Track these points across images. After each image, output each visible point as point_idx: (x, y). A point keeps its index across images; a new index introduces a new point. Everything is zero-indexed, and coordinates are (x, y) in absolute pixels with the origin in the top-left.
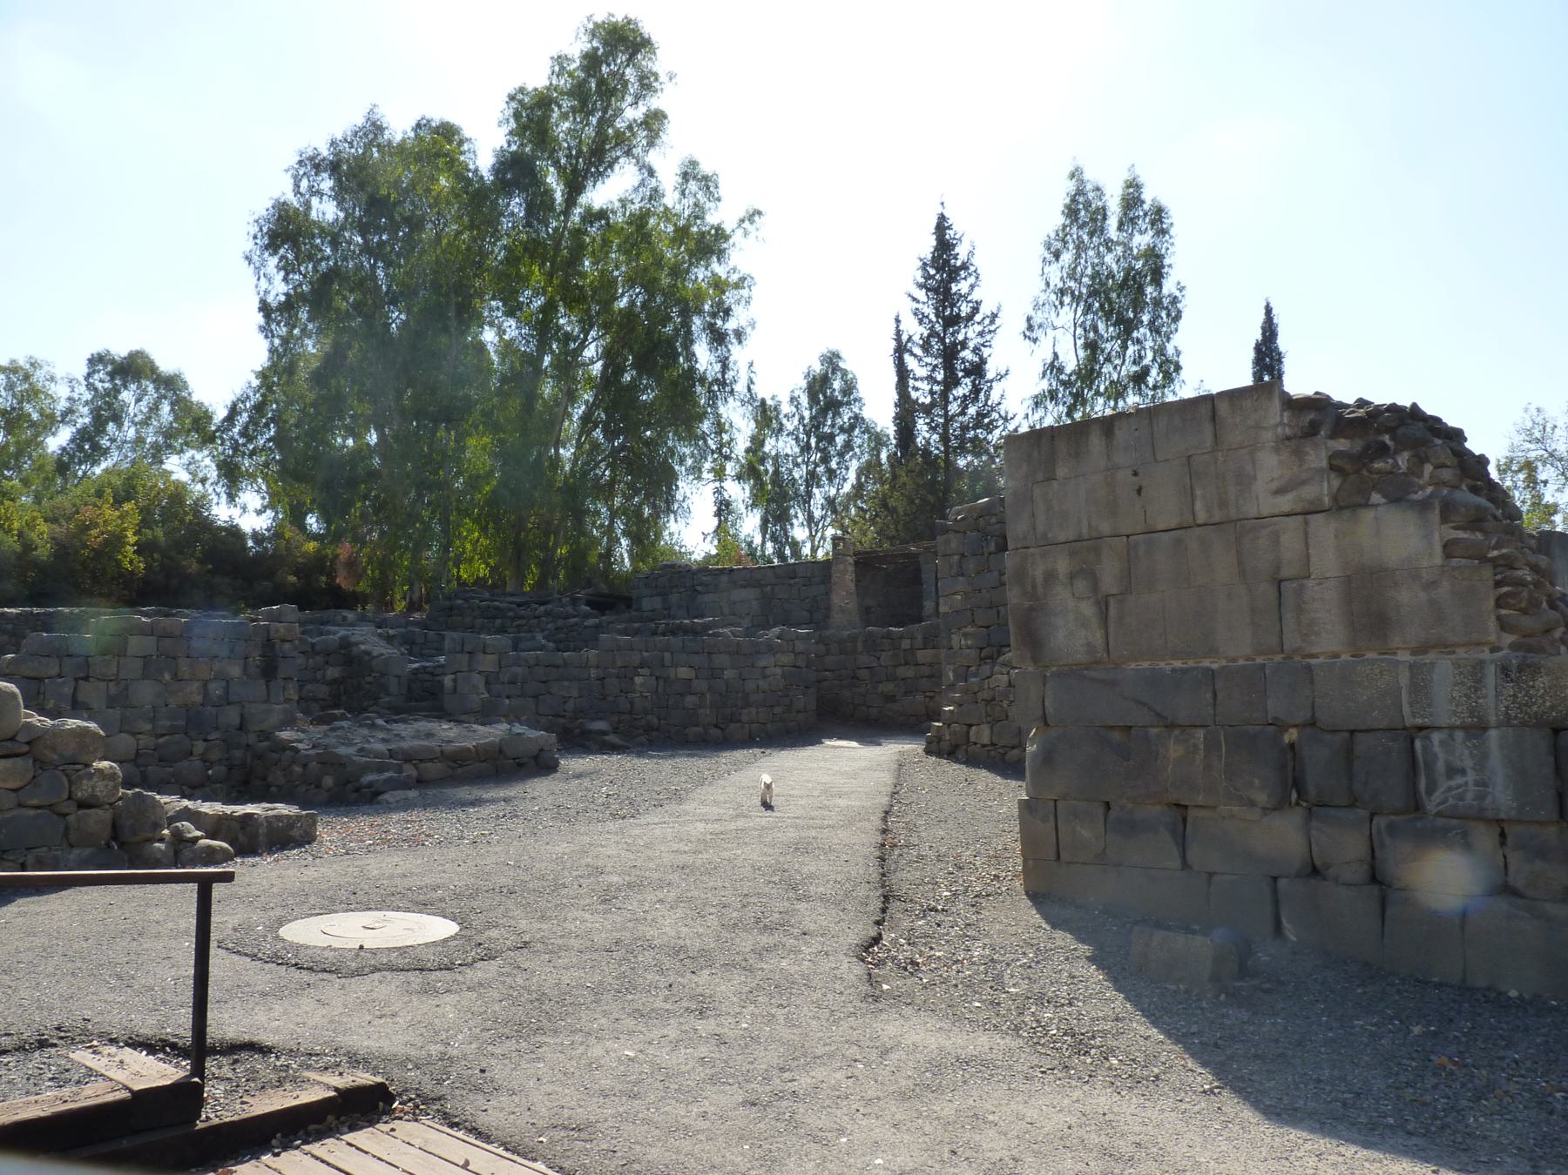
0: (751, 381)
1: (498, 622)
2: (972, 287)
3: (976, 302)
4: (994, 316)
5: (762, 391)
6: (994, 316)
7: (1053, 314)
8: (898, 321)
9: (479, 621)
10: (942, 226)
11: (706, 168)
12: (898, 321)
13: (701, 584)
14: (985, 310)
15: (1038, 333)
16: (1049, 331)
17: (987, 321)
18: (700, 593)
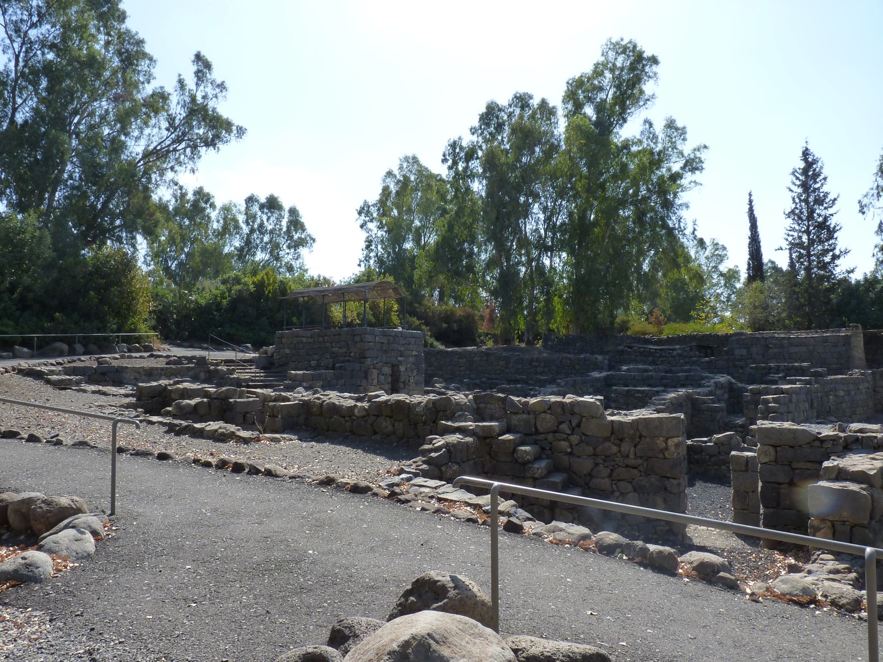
0: (695, 230)
1: (650, 359)
2: (822, 185)
3: (827, 193)
4: (835, 199)
5: (699, 235)
6: (835, 199)
7: (875, 201)
8: (750, 195)
9: (639, 358)
10: (806, 153)
11: (679, 124)
12: (750, 195)
13: (771, 344)
14: (831, 197)
15: (865, 209)
16: (871, 209)
17: (831, 202)
18: (770, 348)
